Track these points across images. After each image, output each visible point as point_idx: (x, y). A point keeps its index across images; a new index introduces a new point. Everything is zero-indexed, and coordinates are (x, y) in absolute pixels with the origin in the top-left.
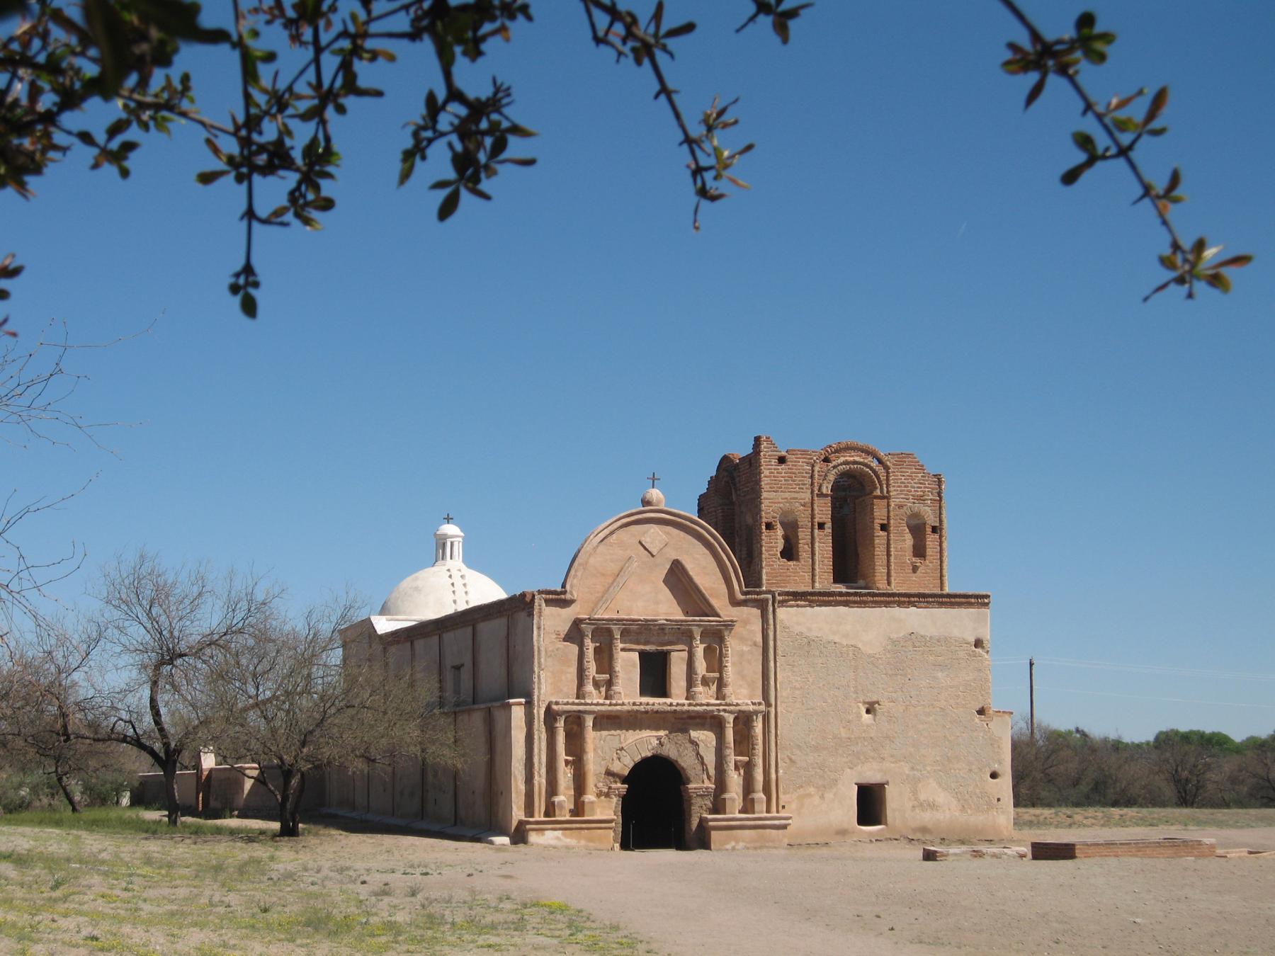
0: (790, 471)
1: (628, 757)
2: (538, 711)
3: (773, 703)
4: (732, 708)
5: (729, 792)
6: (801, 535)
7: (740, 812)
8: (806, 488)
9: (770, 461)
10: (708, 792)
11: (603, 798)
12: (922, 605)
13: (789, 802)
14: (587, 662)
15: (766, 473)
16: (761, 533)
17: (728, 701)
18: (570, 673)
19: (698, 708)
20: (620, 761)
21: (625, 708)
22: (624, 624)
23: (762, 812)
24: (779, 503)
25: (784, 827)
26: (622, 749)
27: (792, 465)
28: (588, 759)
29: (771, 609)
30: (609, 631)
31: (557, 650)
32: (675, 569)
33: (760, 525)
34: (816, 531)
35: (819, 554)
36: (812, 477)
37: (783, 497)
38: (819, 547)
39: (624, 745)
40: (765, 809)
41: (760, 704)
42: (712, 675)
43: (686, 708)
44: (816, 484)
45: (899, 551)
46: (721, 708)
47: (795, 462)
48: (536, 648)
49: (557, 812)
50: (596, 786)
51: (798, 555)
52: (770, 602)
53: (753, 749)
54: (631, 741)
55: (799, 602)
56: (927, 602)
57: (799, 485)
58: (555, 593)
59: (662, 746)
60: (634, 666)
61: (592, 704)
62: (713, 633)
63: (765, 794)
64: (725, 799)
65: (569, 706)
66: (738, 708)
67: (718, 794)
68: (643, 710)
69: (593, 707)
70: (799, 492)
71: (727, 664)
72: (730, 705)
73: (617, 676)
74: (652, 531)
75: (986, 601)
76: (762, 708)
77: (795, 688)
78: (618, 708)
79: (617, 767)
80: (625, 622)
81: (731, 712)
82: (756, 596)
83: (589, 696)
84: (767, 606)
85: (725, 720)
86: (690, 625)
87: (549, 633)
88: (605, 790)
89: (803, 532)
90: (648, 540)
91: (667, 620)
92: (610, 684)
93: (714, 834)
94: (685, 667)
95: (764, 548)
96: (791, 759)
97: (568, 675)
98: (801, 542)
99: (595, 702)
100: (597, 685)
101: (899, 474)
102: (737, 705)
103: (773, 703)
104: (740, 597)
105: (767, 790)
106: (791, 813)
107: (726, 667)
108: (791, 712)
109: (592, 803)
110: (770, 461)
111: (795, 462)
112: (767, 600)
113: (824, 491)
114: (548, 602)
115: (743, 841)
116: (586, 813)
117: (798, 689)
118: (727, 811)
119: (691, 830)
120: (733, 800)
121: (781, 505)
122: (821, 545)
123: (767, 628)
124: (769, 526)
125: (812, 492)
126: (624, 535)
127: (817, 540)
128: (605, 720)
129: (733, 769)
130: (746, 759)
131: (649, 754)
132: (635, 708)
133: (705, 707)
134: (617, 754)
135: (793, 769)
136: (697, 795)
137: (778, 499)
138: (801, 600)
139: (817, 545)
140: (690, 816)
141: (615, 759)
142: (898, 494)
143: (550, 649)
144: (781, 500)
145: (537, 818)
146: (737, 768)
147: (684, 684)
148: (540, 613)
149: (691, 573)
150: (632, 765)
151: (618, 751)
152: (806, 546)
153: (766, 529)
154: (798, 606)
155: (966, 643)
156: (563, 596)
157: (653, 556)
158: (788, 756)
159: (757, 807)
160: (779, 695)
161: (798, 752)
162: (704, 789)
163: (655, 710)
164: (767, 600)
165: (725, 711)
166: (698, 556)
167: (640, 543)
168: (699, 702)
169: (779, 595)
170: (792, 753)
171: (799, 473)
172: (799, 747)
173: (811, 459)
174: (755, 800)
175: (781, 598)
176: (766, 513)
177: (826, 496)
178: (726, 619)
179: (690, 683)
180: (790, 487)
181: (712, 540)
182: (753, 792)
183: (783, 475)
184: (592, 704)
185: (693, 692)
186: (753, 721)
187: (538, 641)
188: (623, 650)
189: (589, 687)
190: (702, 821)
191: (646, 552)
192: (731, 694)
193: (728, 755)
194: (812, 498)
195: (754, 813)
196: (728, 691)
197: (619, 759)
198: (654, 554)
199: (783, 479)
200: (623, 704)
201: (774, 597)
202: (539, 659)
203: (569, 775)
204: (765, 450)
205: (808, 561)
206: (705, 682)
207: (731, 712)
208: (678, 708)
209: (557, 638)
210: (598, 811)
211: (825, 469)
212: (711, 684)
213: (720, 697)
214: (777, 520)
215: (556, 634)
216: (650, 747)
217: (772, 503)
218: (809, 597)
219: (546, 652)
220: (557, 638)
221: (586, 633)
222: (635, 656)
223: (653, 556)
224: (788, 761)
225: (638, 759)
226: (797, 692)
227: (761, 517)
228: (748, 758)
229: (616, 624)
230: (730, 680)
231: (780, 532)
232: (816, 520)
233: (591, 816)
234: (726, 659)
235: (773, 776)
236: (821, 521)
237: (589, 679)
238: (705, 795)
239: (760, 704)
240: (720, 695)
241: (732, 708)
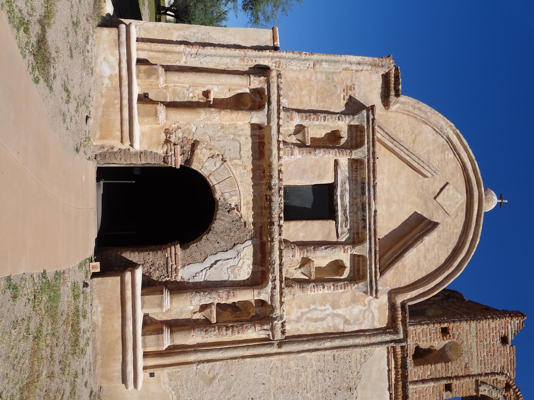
0: (496, 349)
1: (215, 169)
2: (268, 57)
3: (283, 349)
4: (277, 297)
5: (171, 299)
6: (439, 366)
7: (146, 316)
8: (481, 368)
9: (503, 327)
10: (171, 272)
11: (163, 137)
13: (159, 381)
14: (325, 117)
15: (493, 325)
16: (440, 323)
17: (286, 291)
18: (310, 100)
19: (276, 253)
20: (209, 158)
21: (274, 160)
22: (369, 160)
23: (144, 346)
24: (467, 340)
25: (124, 380)
26: (224, 161)
27: (501, 351)
28: (212, 112)
29: (388, 338)
30: (358, 145)
31: (335, 86)
32: (424, 223)
33: (447, 322)
34: (445, 382)
35: (423, 388)
36: (493, 374)
37: (473, 343)
38: (429, 387)
39: (228, 162)
40: (149, 349)
41: (283, 332)
42: (313, 270)
43: (276, 236)
44: (487, 378)
46: (278, 283)
47: (504, 355)
48: (337, 58)
49: (143, 67)
50: (179, 128)
51: (420, 365)
52: (395, 337)
53: (227, 328)
54: (234, 172)
55: (393, 372)
57: (484, 361)
58: (397, 83)
59: (229, 212)
60: (320, 176)
61: (279, 118)
62: (358, 270)
63: (169, 348)
64: (162, 294)
65: (276, 91)
66: (278, 304)
67: (169, 285)
68: (273, 183)
69: (276, 120)
70: (478, 361)
71: (326, 288)
72: (281, 294)
73: (310, 153)
74: (460, 196)
76: (279, 336)
77: (299, 376)
78: (275, 151)
79: (201, 153)
80: (372, 161)
81: (272, 296)
82: (400, 319)
83: (288, 116)
84: (390, 333)
85: (262, 288)
86: (370, 239)
87: (352, 78)
88: (173, 139)
89: (442, 367)
90: (451, 192)
91: (375, 211)
92: (302, 145)
93: (114, 281)
94: (319, 238)
95: (425, 326)
96: (214, 378)
97: (307, 98)
98: (433, 366)
99: (281, 122)
100: (300, 129)
102: (282, 303)
103: (283, 349)
104: (399, 300)
105: (173, 350)
106: (143, 386)
107: (324, 288)
108: (270, 374)
109: (156, 115)
110: (503, 327)
111: (504, 355)
112: (396, 332)
113: (481, 388)
114: (386, 77)
115: (103, 322)
116: (140, 105)
117: (297, 380)
118: (146, 297)
119: (121, 253)
120: (161, 305)
121: (465, 343)
122: (432, 388)
123: (366, 336)
124: (445, 332)
125: (480, 375)
126: (454, 165)
127: (437, 384)
128: (258, 141)
129: (203, 302)
130: (214, 320)
131: (217, 196)
132: (275, 174)
133: (278, 262)
134: (218, 155)
135: (201, 382)
136: (167, 258)
137: (471, 339)
138: (396, 374)
139: (432, 384)
140: (140, 251)
141: (212, 152)
143: (336, 79)
144: (469, 342)
145: (134, 45)
146: (203, 308)
147: (301, 237)
148: (375, 66)
149: (426, 239)
150: (204, 173)
151: (221, 157)
152: (429, 373)
153: (442, 328)
154: (389, 371)
156: (393, 93)
157: (435, 198)
158: (217, 374)
159: (151, 338)
160: (293, 356)
161: (222, 388)
162: (175, 266)
163: (274, 199)
164: (396, 332)
165: (274, 288)
166: (436, 250)
167: (447, 183)
168: (284, 253)
169: (402, 347)
170: (222, 379)
172: (228, 388)
173: (508, 371)
174: (160, 336)
175: (399, 350)
176: (457, 326)
177: (477, 390)
178: (379, 283)
179: (303, 245)
181: (456, 264)
182: (172, 332)
183: (492, 343)
184: (279, 118)
185: (295, 247)
186: (262, 324)
187: (345, 62)
188: (336, 163)
189: (297, 120)
190: (133, 266)
191: (438, 191)
192: (294, 295)
193: (219, 296)
194: (475, 375)
195: (143, 334)
196: (296, 288)
197: (212, 157)
198: (437, 199)
199: (488, 342)
200: (279, 158)
201: (400, 341)
202: (326, 61)
203: (191, 95)
204: (513, 322)
205: (415, 377)
206: (306, 261)
207: (272, 296)
208: (276, 228)
209: (347, 86)
210: (146, 128)
211: (500, 386)
212: (302, 270)
213: (288, 281)
214: (452, 340)
215: (351, 86)
216: (227, 195)
217: (467, 332)
218: (400, 383)
219: (333, 73)
220: (347, 86)
221: (356, 117)
222: (329, 180)
223: (435, 198)
224: (211, 375)
225: (212, 181)
226: (294, 379)
227: (454, 322)
228: (215, 322)
229: (368, 151)
230: (309, 292)
231: (438, 344)
232: (455, 382)
233: (139, 114)
234: (332, 287)
235: (192, 357)
236: (453, 386)
237: (306, 118)
238: (167, 270)
239: (283, 332)
240: (290, 282)
241: (277, 297)
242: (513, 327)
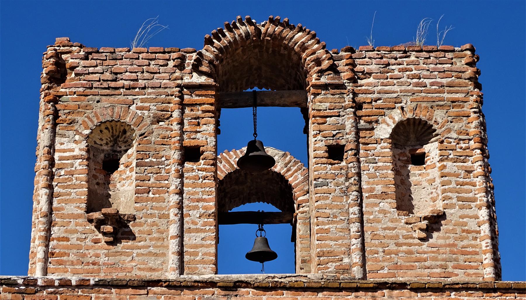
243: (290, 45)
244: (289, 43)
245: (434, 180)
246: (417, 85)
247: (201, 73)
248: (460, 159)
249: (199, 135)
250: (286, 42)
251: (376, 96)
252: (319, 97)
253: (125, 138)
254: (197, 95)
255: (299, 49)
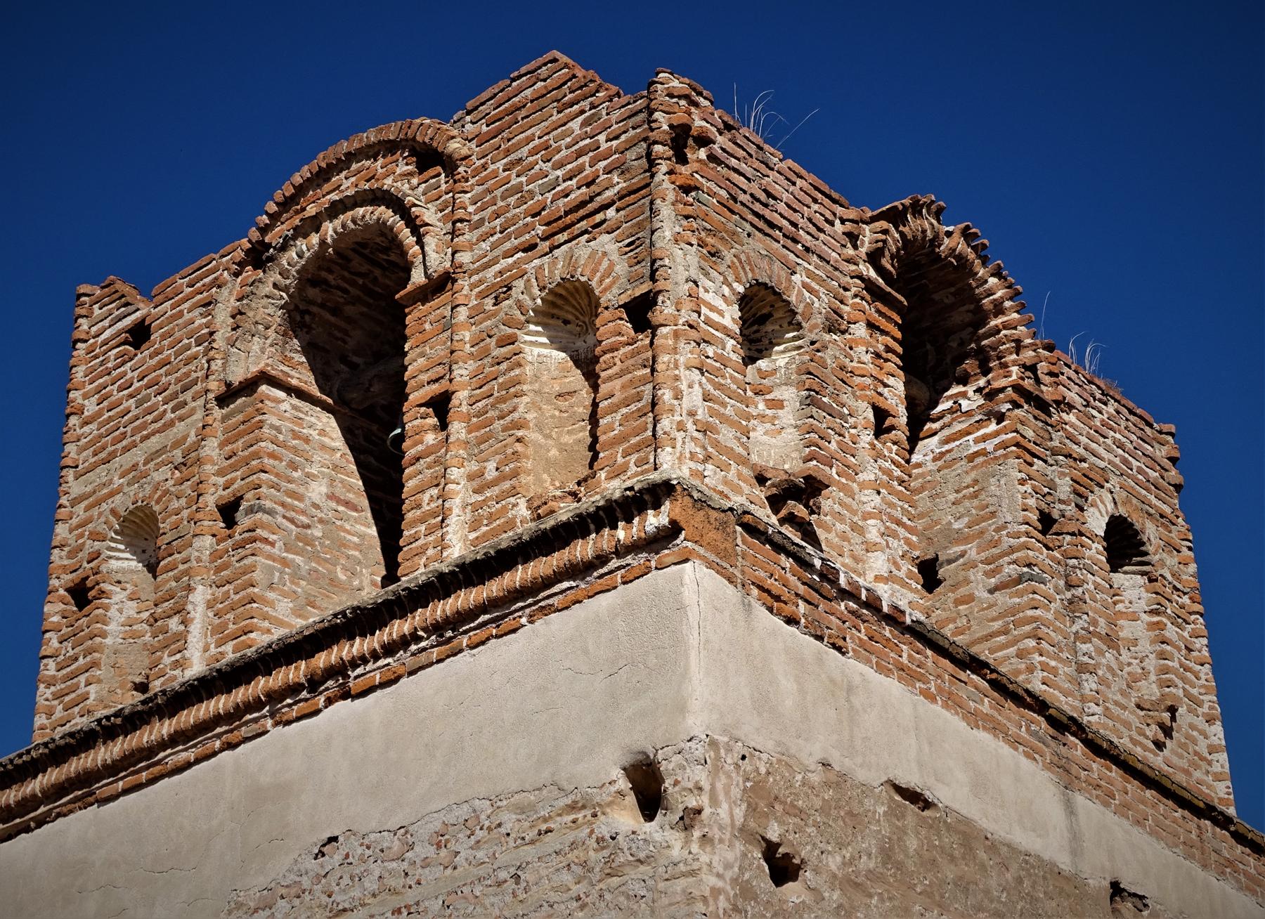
9: (102, 363)
12: (373, 672)
45: (490, 485)
56: (390, 649)
75: (654, 520)
101: (500, 165)
142: (494, 247)
155: (573, 807)
171: (177, 355)
180: (150, 418)
242: (106, 323)
243: (977, 291)
244: (977, 287)
245: (1135, 642)
246: (1125, 461)
247: (880, 270)
248: (1180, 620)
249: (885, 391)
250: (974, 285)
251: (1081, 451)
252: (1017, 411)
253: (756, 332)
254: (878, 311)
255: (991, 307)
